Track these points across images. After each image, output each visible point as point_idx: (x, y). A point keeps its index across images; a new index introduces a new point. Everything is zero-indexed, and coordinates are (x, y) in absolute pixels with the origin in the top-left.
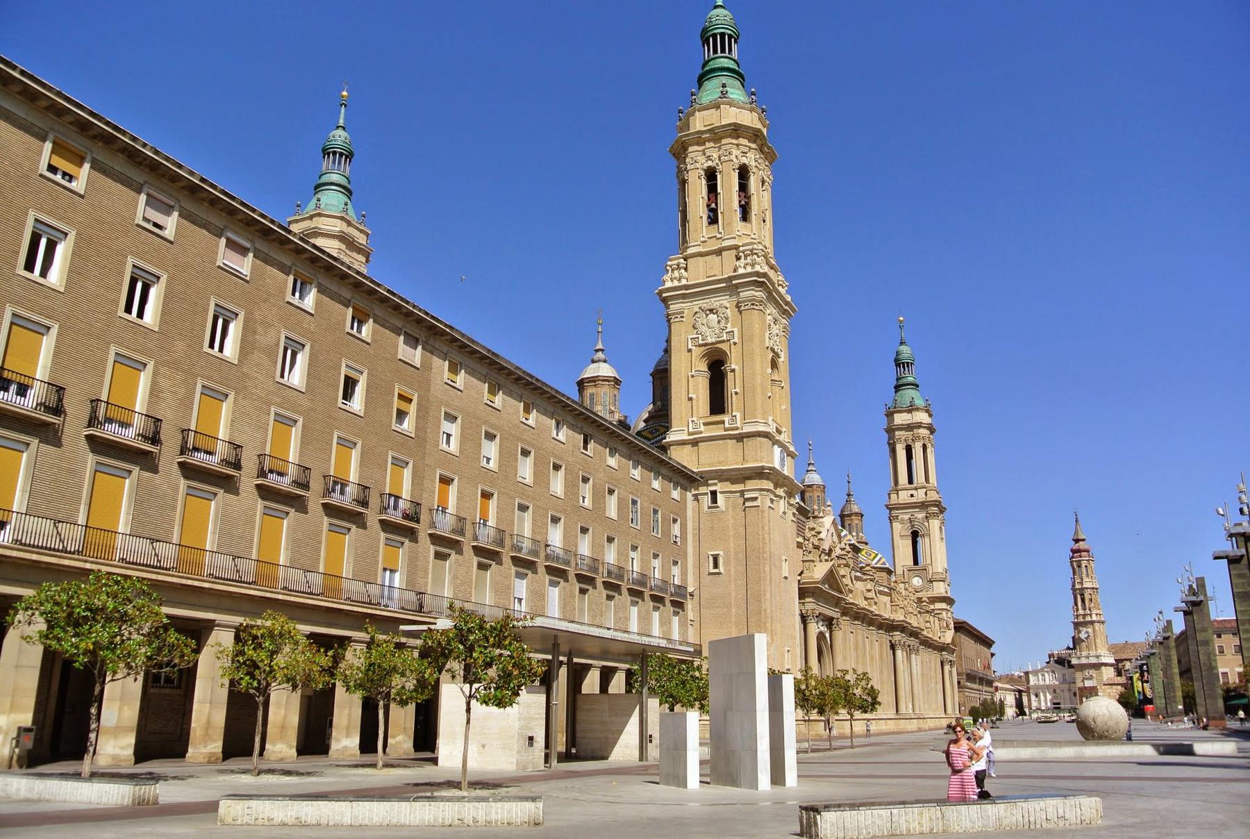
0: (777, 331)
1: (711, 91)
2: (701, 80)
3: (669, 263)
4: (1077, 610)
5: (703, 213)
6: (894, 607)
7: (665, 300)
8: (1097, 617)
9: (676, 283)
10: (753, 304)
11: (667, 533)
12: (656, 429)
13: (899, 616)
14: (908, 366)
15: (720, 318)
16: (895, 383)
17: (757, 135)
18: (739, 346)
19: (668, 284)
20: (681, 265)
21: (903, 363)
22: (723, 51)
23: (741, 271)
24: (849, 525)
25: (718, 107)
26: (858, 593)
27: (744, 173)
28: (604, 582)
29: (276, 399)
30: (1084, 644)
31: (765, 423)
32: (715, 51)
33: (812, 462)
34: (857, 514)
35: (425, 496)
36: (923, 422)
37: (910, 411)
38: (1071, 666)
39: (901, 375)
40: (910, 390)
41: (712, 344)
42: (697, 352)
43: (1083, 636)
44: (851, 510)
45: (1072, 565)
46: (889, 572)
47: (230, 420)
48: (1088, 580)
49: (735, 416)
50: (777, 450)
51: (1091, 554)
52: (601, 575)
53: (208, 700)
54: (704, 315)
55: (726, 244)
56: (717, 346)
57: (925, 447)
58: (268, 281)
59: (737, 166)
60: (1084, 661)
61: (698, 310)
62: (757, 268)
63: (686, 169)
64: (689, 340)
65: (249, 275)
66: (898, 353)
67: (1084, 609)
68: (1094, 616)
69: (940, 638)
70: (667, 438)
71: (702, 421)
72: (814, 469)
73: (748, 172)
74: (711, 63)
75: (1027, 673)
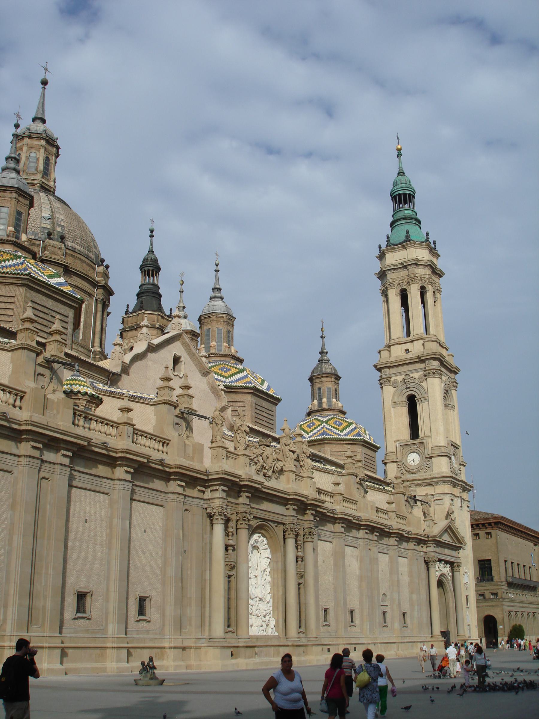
6: (215, 451)
16: (391, 219)
21: (399, 195)
33: (218, 286)
34: (328, 375)
44: (321, 371)
46: (374, 448)
57: (423, 291)
66: (395, 184)
72: (218, 294)
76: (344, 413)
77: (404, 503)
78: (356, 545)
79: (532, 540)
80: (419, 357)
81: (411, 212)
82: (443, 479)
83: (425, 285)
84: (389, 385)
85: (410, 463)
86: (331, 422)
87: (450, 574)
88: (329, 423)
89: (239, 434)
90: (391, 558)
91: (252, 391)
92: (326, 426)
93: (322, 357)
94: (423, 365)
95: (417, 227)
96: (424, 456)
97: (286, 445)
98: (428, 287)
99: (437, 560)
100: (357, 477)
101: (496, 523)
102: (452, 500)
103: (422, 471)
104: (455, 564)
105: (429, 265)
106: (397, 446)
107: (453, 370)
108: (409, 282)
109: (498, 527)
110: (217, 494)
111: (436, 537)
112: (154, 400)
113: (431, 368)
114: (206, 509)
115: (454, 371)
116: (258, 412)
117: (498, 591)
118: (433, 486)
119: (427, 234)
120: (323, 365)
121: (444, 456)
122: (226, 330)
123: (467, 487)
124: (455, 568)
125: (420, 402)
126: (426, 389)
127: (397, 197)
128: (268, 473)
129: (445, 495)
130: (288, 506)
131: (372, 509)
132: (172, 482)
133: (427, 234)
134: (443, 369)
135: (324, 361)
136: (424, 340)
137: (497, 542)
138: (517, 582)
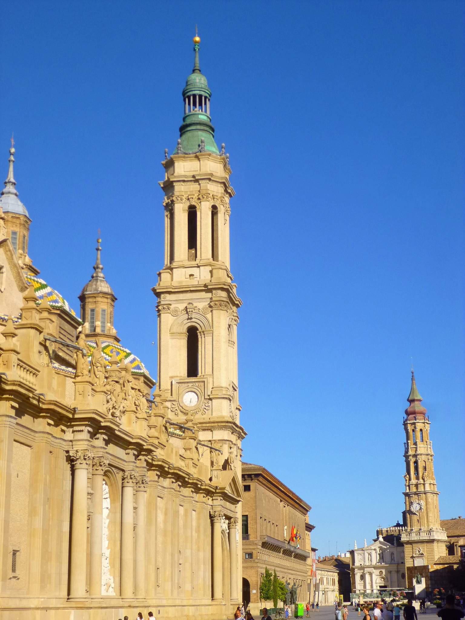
4: (410, 480)
6: (80, 387)
8: (430, 487)
14: (200, 104)
21: (194, 96)
24: (93, 310)
30: (415, 518)
33: (12, 180)
36: (214, 173)
37: (197, 157)
38: (401, 544)
39: (190, 111)
40: (200, 133)
43: (415, 508)
44: (96, 290)
51: (426, 417)
57: (214, 210)
67: (418, 478)
68: (427, 486)
69: (211, 479)
75: (352, 553)
77: (194, 449)
78: (162, 496)
79: (280, 496)
80: (205, 286)
82: (224, 424)
83: (217, 205)
84: (169, 313)
85: (186, 404)
86: (107, 350)
87: (228, 531)
88: (105, 351)
89: (97, 367)
90: (186, 511)
91: (58, 312)
94: (209, 295)
95: (211, 136)
96: (203, 397)
97: (129, 382)
98: (220, 207)
99: (223, 514)
100: (164, 418)
101: (257, 475)
102: (231, 448)
103: (200, 413)
104: (232, 520)
106: (173, 383)
107: (236, 302)
108: (199, 199)
109: (258, 480)
110: (79, 436)
111: (225, 489)
112: (18, 323)
114: (67, 452)
115: (238, 304)
117: (253, 551)
118: (212, 431)
120: (99, 283)
121: (226, 398)
122: (22, 234)
123: (243, 434)
124: (232, 524)
125: (203, 336)
126: (211, 322)
127: (192, 98)
128: (116, 413)
129: (224, 442)
130: (128, 451)
131: (176, 455)
132: (40, 420)
135: (99, 278)
136: (213, 267)
138: (271, 541)
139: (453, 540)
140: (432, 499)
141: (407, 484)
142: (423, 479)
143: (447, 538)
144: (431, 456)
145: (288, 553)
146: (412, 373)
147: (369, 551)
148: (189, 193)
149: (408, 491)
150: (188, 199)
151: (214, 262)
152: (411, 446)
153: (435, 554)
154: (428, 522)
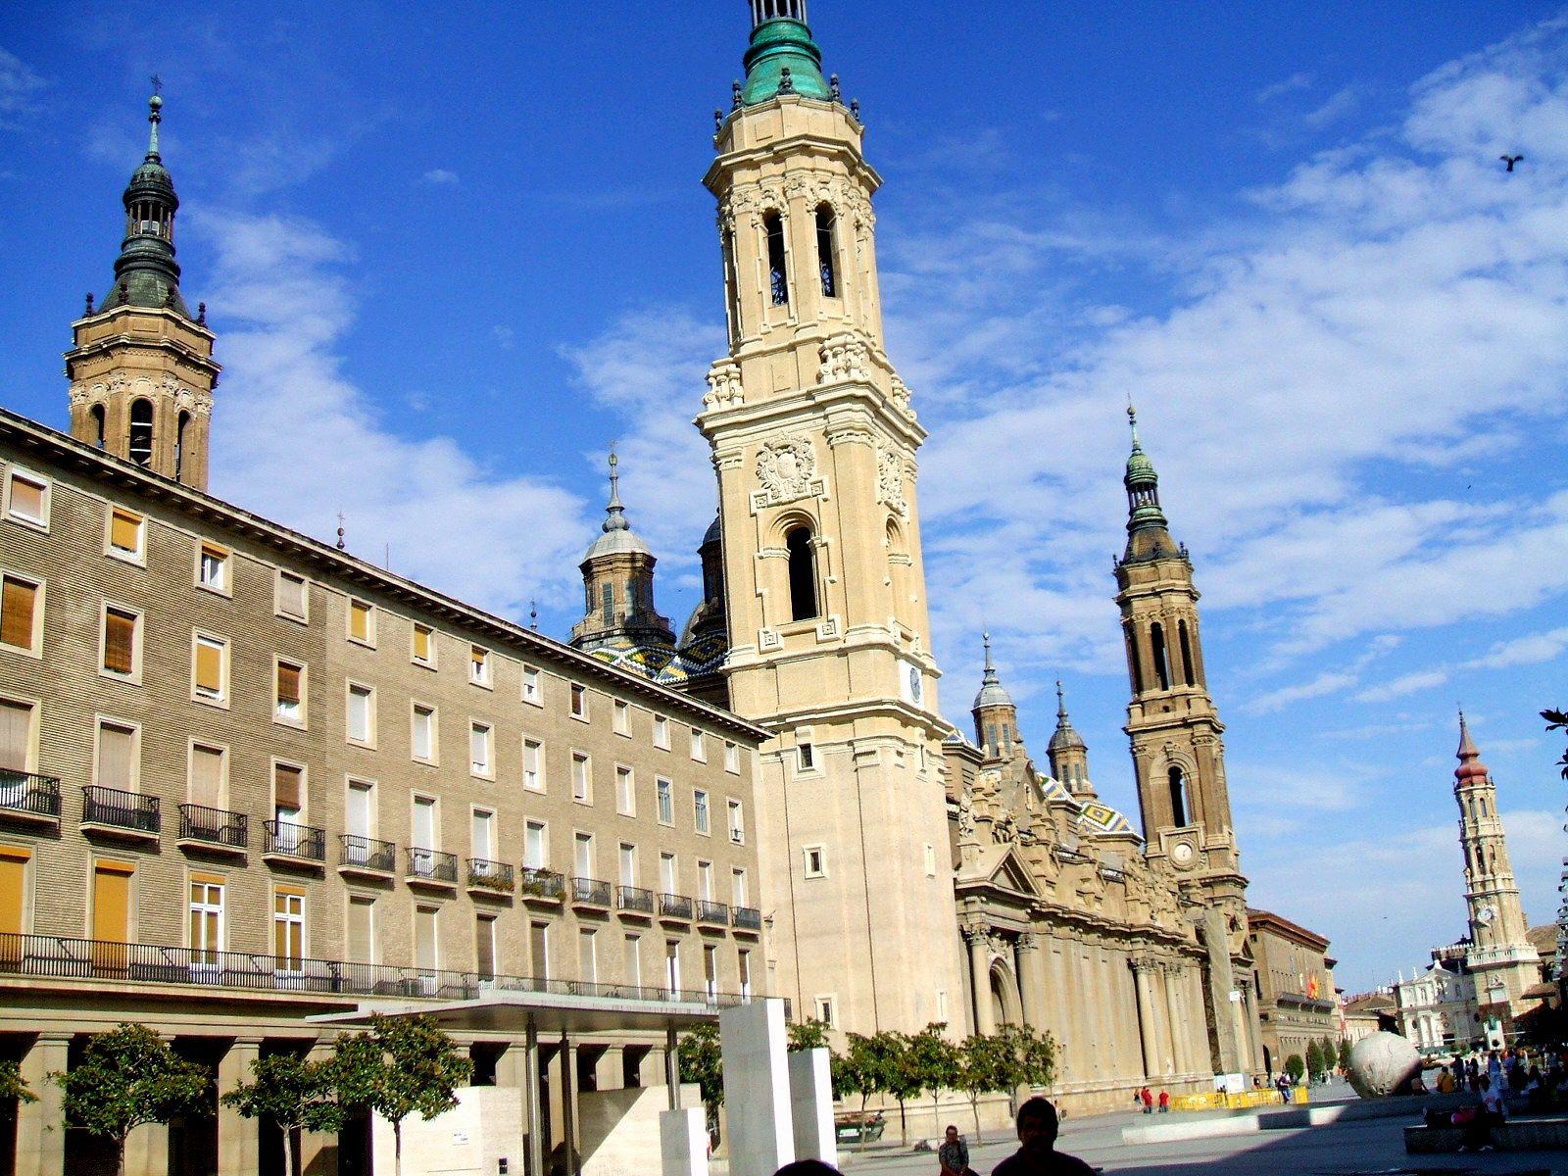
0: (897, 474)
1: (764, 80)
2: (751, 58)
3: (712, 372)
4: (1472, 875)
5: (762, 286)
7: (708, 434)
8: (1504, 884)
9: (726, 406)
10: (851, 434)
11: (720, 827)
12: (711, 645)
13: (1140, 917)
15: (798, 460)
17: (844, 152)
18: (833, 503)
19: (713, 408)
20: (732, 375)
22: (783, 11)
23: (828, 380)
24: (1065, 767)
25: (778, 106)
26: (1060, 891)
27: (825, 215)
28: (620, 916)
29: (101, 702)
30: (1485, 932)
31: (881, 628)
32: (769, 13)
35: (330, 815)
38: (1469, 971)
41: (790, 502)
42: (766, 516)
43: (1482, 918)
45: (1459, 800)
47: (38, 742)
48: (1486, 823)
49: (833, 620)
50: (905, 667)
51: (1489, 780)
52: (614, 905)
53: (38, 1146)
54: (774, 456)
55: (801, 336)
56: (797, 505)
58: (77, 529)
59: (813, 206)
60: (1487, 960)
61: (763, 448)
62: (855, 375)
63: (731, 213)
64: (753, 500)
65: (48, 526)
66: (1129, 470)
67: (1483, 872)
68: (1499, 883)
70: (726, 663)
71: (780, 632)
72: (994, 679)
73: (832, 214)
74: (764, 32)
75: (1396, 989)
76: (1095, 796)
81: (1155, 511)
88: (1088, 814)
91: (1064, 806)
92: (1087, 819)
93: (1061, 721)
94: (1188, 731)
101: (1263, 923)
103: (1197, 868)
105: (1188, 591)
113: (1201, 734)
116: (1070, 829)
119: (1181, 544)
133: (1181, 544)
134: (1213, 734)
137: (1264, 948)
139: (1548, 959)
140: (1509, 901)
141: (1469, 882)
142: (1492, 873)
143: (1537, 958)
144: (1501, 837)
145: (1307, 1007)
146: (1461, 714)
147: (1421, 986)
148: (1150, 609)
149: (1471, 892)
150: (1150, 617)
151: (1191, 689)
152: (1469, 824)
153: (1522, 982)
154: (1505, 936)
